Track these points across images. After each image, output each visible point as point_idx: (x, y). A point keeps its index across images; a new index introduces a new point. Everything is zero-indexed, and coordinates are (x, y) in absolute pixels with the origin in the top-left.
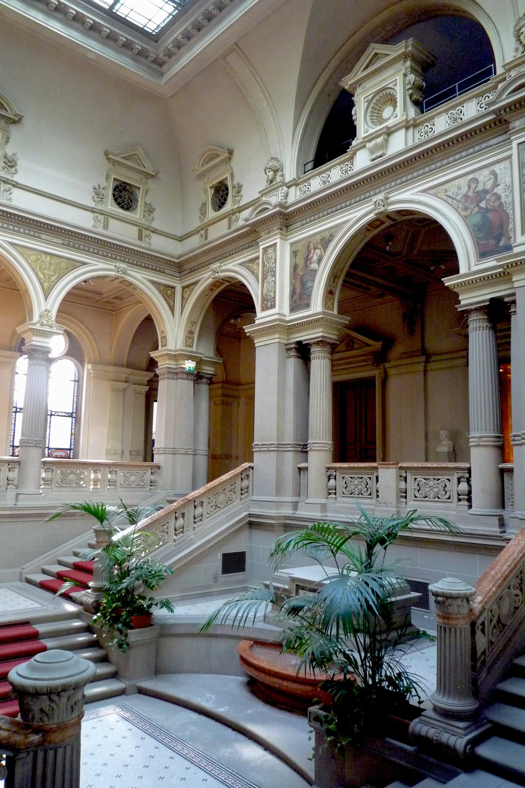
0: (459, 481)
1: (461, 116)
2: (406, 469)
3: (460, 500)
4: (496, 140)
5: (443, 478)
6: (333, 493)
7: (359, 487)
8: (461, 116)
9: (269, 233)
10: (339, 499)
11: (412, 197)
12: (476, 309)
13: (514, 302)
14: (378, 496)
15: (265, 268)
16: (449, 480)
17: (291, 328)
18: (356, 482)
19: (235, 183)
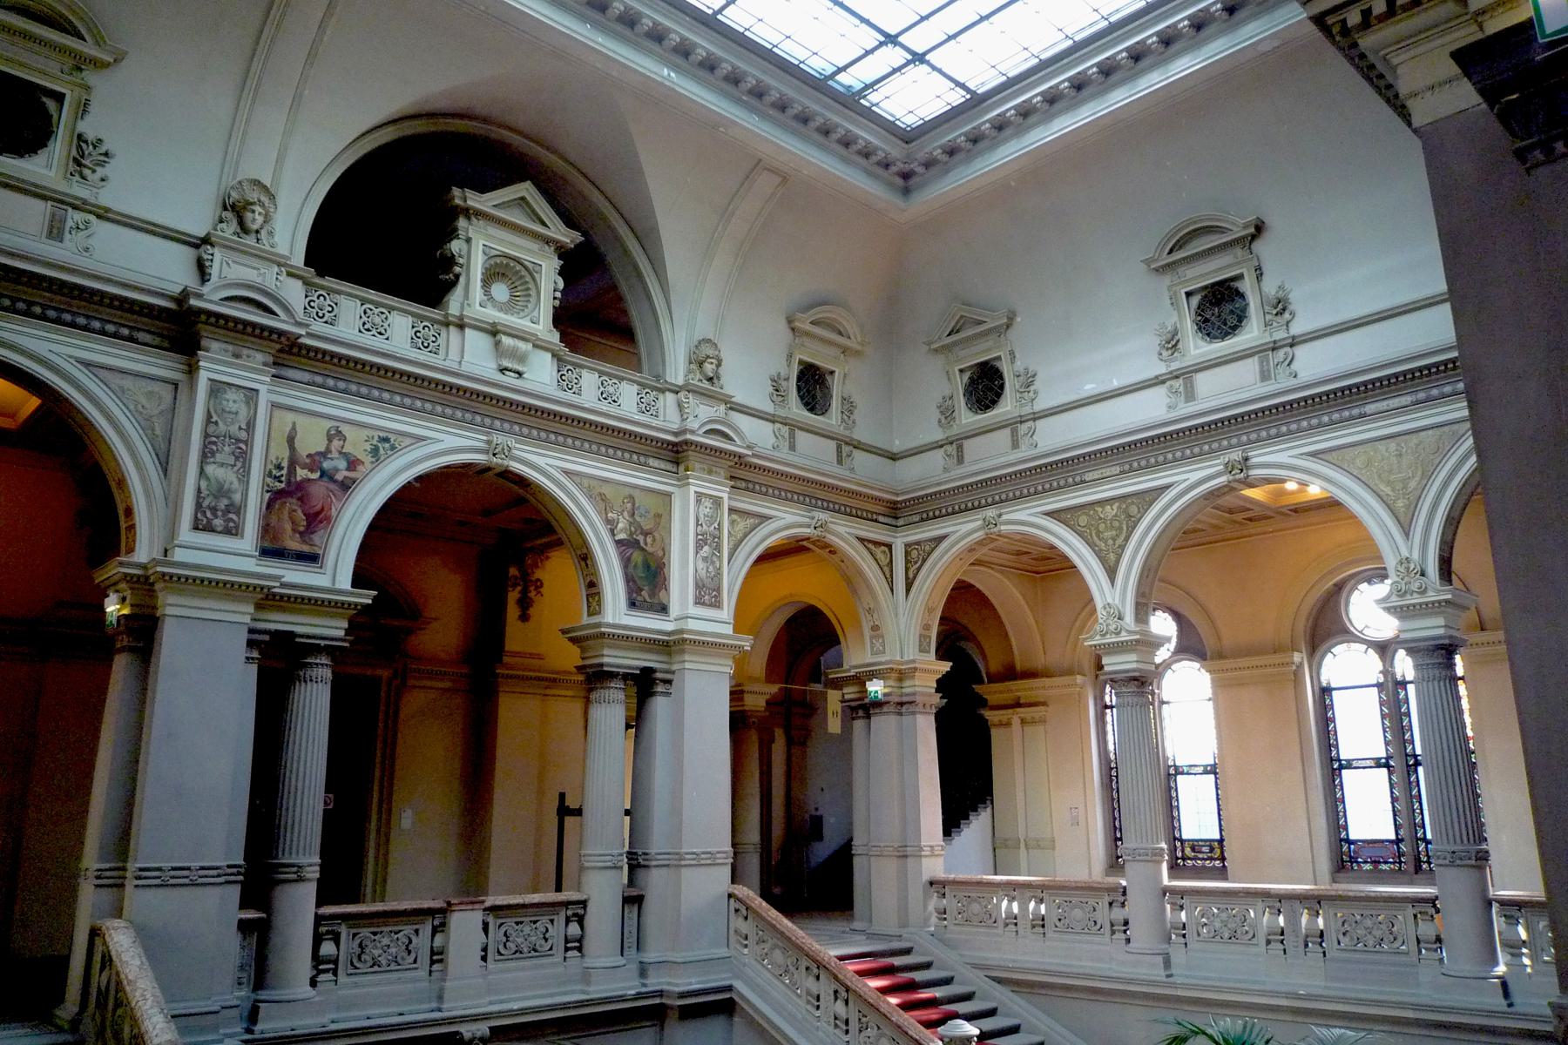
0: (568, 921)
2: (494, 909)
3: (567, 949)
4: (663, 465)
5: (545, 920)
6: (327, 971)
7: (393, 950)
9: (237, 356)
10: (342, 978)
11: (543, 464)
12: (626, 677)
13: (669, 682)
14: (433, 962)
15: (211, 429)
16: (552, 921)
17: (269, 599)
18: (386, 941)
19: (87, 127)
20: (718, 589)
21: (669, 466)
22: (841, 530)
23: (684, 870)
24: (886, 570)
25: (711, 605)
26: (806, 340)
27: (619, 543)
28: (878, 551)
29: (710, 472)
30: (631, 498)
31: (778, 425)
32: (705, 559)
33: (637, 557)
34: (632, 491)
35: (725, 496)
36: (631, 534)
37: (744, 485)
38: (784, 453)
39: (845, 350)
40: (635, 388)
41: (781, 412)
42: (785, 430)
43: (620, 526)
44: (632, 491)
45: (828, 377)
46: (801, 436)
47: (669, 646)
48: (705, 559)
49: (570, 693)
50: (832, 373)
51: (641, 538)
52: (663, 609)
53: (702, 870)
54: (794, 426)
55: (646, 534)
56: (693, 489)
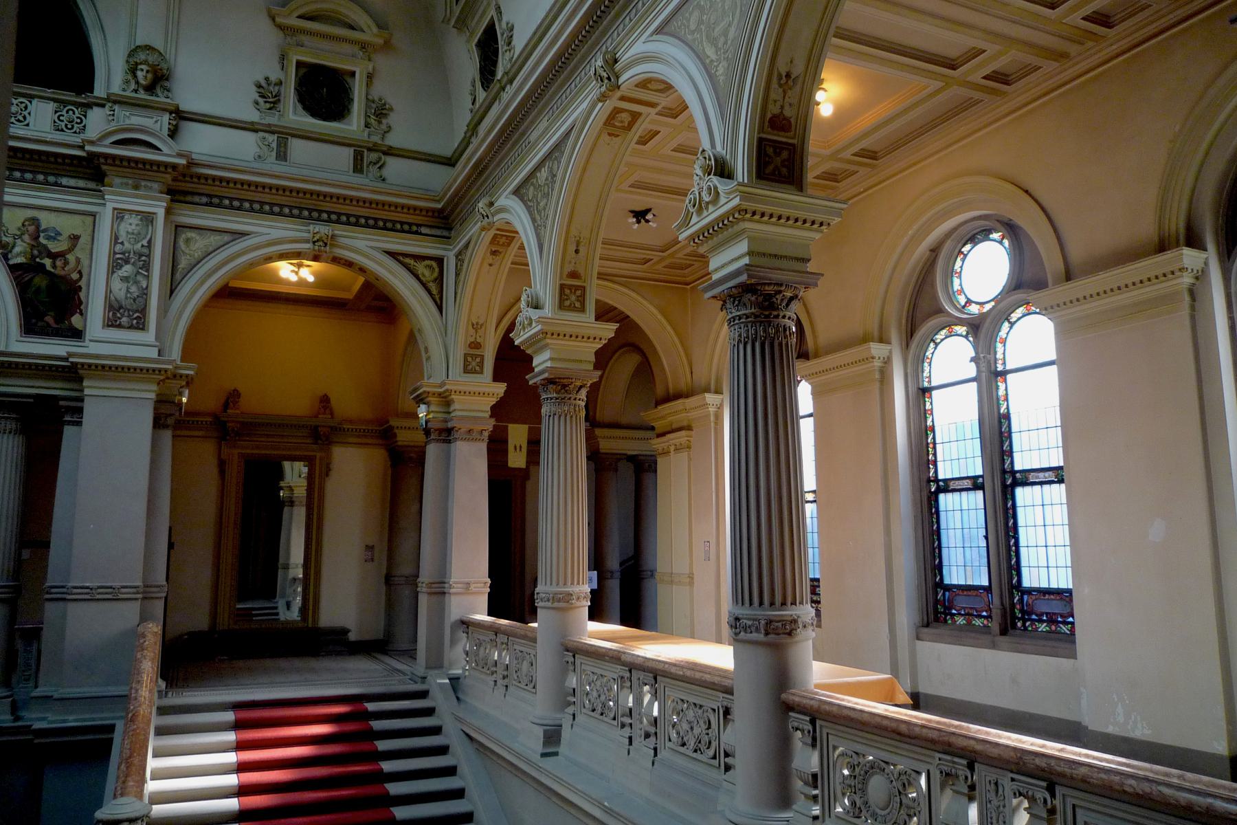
1: (26, 113)
8: (26, 113)
20: (143, 311)
21: (91, 185)
22: (360, 244)
23: (71, 606)
24: (434, 288)
25: (131, 327)
26: (304, 39)
27: (13, 269)
28: (421, 268)
29: (136, 187)
30: (35, 221)
31: (261, 134)
32: (125, 279)
33: (40, 281)
34: (30, 213)
35: (161, 212)
36: (33, 257)
37: (204, 200)
38: (271, 164)
39: (363, 46)
40: (51, 106)
41: (272, 119)
42: (272, 138)
43: (17, 249)
44: (30, 213)
45: (349, 79)
46: (296, 145)
47: (72, 373)
48: (125, 279)
49: (200, 433)
50: (353, 74)
51: (47, 262)
52: (77, 334)
53: (93, 605)
54: (284, 136)
55: (54, 256)
56: (110, 206)
